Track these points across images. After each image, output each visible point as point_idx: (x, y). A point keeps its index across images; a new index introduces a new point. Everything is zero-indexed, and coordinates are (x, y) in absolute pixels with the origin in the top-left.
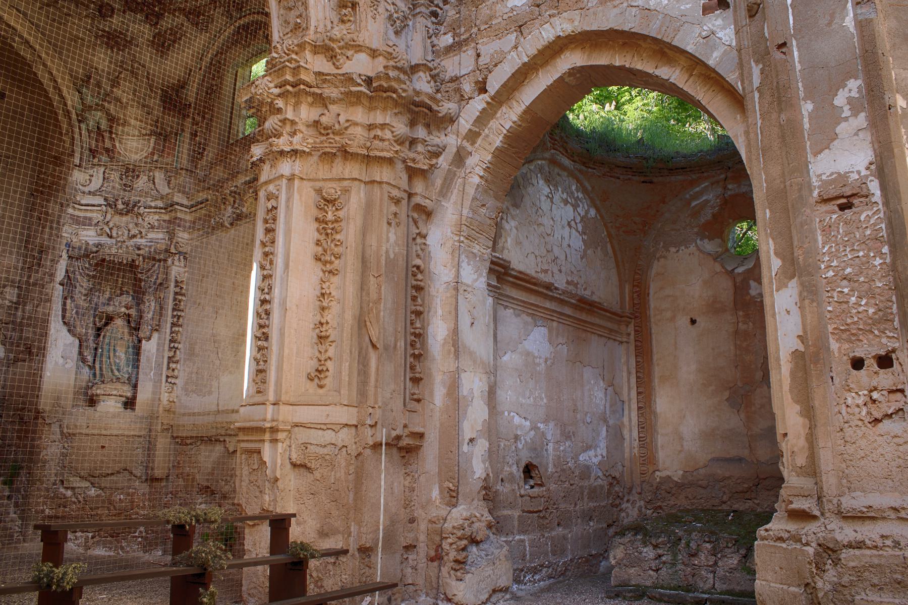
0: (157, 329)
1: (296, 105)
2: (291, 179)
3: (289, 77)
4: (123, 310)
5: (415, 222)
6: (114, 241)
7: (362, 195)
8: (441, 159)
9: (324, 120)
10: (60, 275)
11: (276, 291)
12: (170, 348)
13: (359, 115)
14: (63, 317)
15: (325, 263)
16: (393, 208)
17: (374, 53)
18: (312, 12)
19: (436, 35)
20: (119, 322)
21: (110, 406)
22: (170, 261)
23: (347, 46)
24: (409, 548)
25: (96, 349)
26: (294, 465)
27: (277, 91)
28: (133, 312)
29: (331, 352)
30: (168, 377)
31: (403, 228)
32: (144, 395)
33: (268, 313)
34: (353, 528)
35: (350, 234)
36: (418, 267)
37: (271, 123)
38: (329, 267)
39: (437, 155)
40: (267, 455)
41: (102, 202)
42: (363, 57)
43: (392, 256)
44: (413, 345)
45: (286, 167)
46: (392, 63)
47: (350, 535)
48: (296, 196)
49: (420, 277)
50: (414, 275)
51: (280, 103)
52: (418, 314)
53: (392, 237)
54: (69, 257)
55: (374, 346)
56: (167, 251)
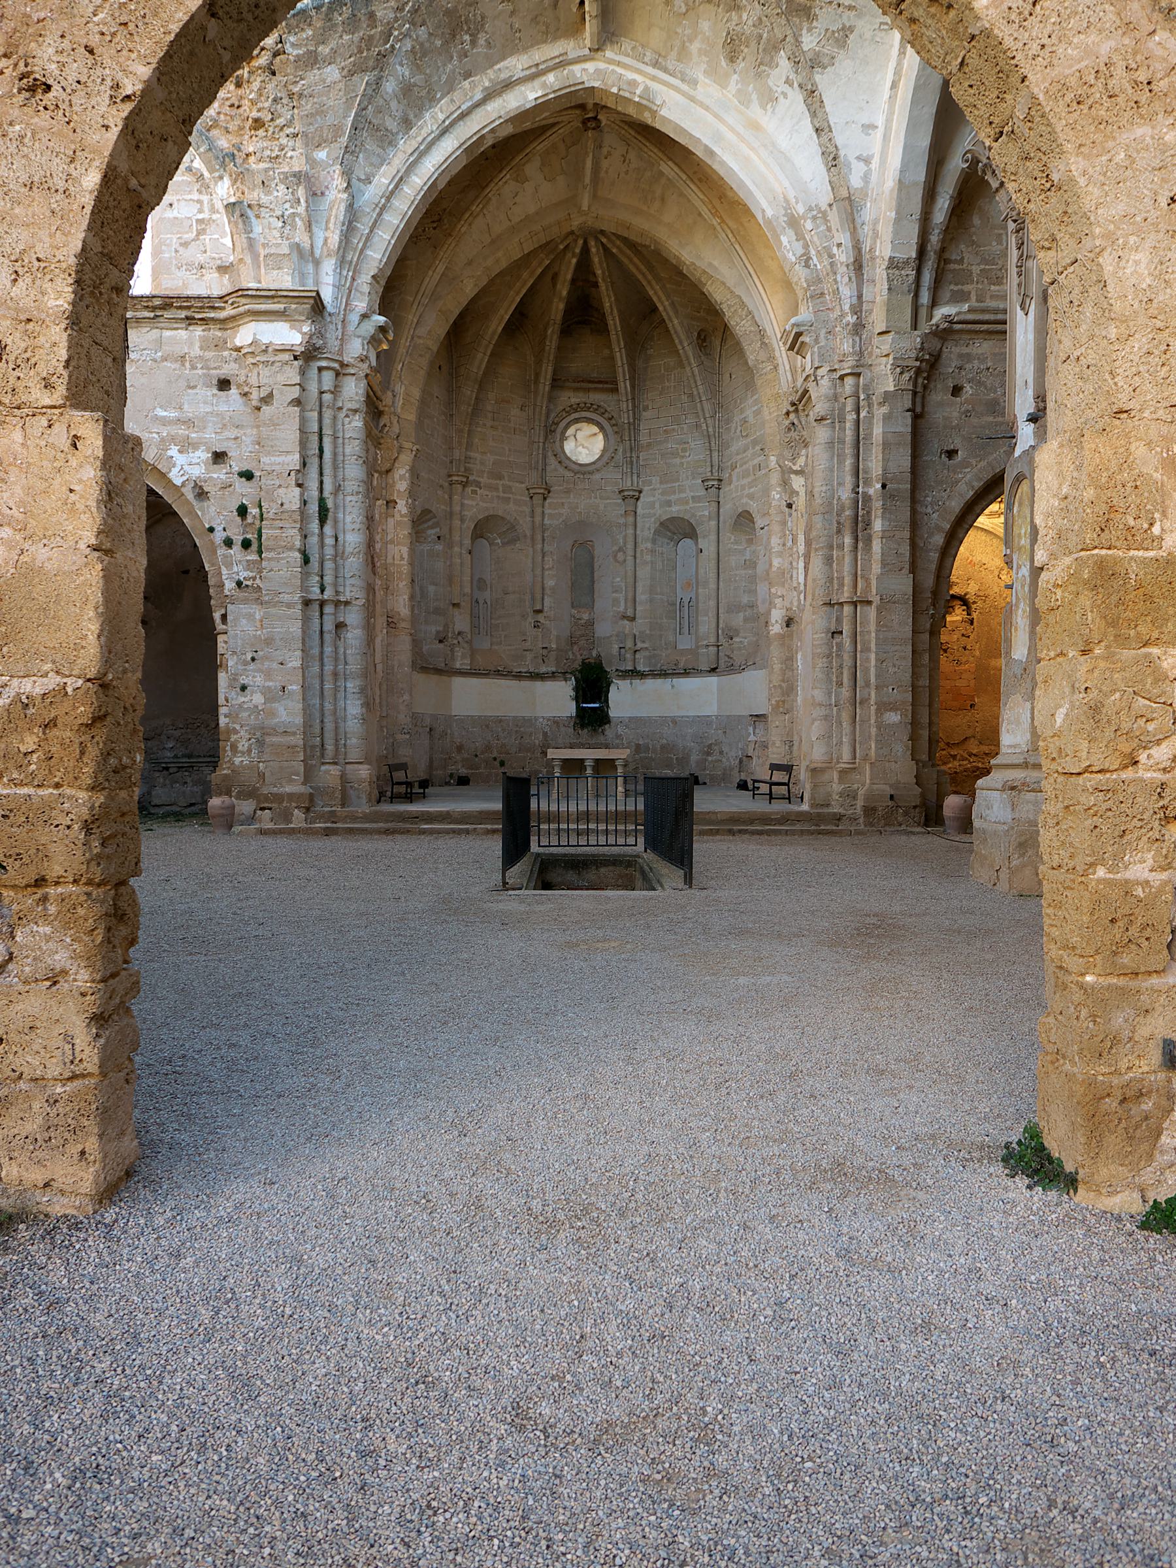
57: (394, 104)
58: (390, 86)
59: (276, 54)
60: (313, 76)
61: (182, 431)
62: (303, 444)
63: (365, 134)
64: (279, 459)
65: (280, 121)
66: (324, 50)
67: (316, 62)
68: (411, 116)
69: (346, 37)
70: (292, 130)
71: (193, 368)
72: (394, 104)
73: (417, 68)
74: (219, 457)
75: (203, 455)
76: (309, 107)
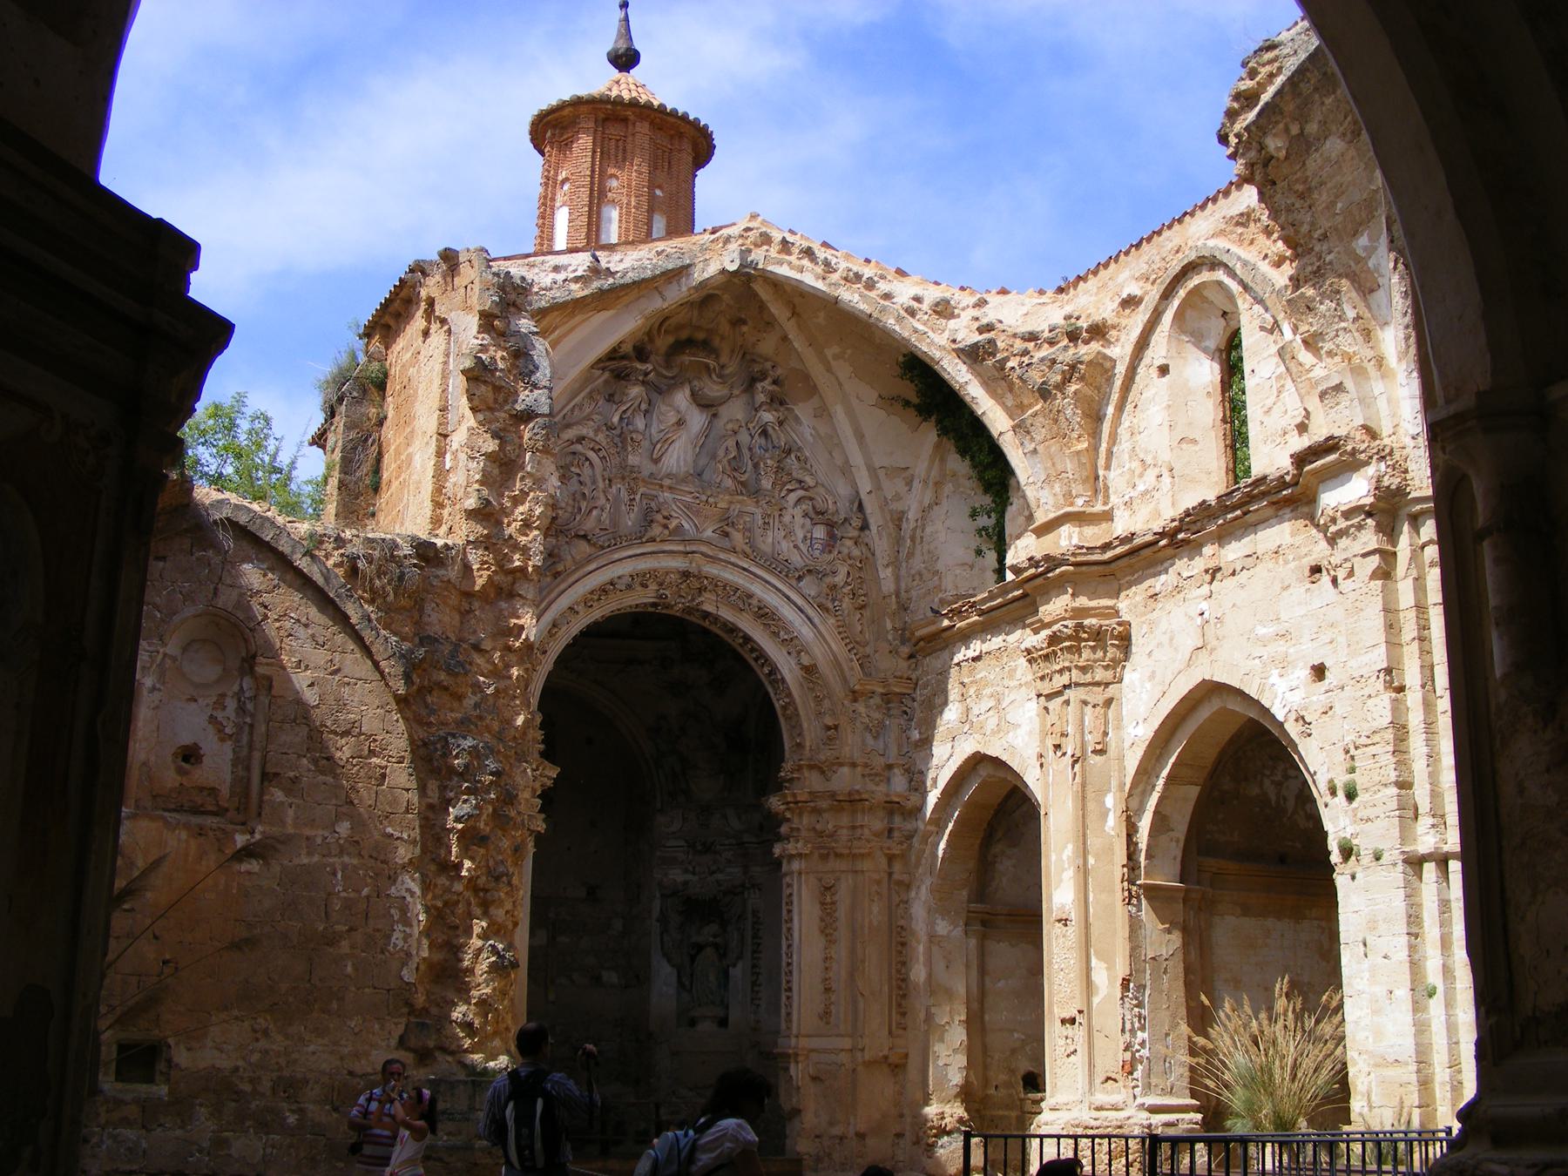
0: (740, 957)
1: (800, 815)
2: (800, 873)
4: (711, 939)
5: (898, 893)
6: (695, 878)
7: (850, 881)
8: (915, 839)
9: (818, 827)
10: (656, 913)
11: (795, 957)
12: (753, 974)
13: (845, 820)
14: (662, 948)
15: (827, 935)
16: (875, 887)
17: (854, 765)
18: (806, 733)
19: (909, 729)
20: (709, 951)
21: (706, 1027)
22: (746, 893)
23: (833, 764)
24: (899, 1135)
25: (692, 975)
26: (815, 1079)
27: (782, 807)
28: (718, 940)
29: (833, 999)
30: (752, 999)
32: (735, 1015)
33: (791, 972)
34: (852, 1120)
35: (842, 911)
36: (902, 927)
37: (784, 829)
38: (829, 938)
39: (912, 837)
40: (793, 1071)
41: (683, 843)
42: (845, 770)
43: (875, 924)
44: (900, 988)
45: (796, 865)
46: (867, 771)
48: (804, 887)
49: (904, 934)
50: (899, 933)
51: (788, 815)
52: (904, 963)
53: (875, 909)
54: (662, 895)
55: (861, 994)
56: (743, 886)
59: (1266, 165)
60: (1313, 162)
61: (1280, 647)
62: (1392, 627)
64: (1365, 659)
65: (1305, 228)
66: (1312, 128)
67: (1309, 145)
69: (1329, 101)
70: (1319, 232)
71: (1286, 562)
74: (1319, 672)
75: (1304, 673)
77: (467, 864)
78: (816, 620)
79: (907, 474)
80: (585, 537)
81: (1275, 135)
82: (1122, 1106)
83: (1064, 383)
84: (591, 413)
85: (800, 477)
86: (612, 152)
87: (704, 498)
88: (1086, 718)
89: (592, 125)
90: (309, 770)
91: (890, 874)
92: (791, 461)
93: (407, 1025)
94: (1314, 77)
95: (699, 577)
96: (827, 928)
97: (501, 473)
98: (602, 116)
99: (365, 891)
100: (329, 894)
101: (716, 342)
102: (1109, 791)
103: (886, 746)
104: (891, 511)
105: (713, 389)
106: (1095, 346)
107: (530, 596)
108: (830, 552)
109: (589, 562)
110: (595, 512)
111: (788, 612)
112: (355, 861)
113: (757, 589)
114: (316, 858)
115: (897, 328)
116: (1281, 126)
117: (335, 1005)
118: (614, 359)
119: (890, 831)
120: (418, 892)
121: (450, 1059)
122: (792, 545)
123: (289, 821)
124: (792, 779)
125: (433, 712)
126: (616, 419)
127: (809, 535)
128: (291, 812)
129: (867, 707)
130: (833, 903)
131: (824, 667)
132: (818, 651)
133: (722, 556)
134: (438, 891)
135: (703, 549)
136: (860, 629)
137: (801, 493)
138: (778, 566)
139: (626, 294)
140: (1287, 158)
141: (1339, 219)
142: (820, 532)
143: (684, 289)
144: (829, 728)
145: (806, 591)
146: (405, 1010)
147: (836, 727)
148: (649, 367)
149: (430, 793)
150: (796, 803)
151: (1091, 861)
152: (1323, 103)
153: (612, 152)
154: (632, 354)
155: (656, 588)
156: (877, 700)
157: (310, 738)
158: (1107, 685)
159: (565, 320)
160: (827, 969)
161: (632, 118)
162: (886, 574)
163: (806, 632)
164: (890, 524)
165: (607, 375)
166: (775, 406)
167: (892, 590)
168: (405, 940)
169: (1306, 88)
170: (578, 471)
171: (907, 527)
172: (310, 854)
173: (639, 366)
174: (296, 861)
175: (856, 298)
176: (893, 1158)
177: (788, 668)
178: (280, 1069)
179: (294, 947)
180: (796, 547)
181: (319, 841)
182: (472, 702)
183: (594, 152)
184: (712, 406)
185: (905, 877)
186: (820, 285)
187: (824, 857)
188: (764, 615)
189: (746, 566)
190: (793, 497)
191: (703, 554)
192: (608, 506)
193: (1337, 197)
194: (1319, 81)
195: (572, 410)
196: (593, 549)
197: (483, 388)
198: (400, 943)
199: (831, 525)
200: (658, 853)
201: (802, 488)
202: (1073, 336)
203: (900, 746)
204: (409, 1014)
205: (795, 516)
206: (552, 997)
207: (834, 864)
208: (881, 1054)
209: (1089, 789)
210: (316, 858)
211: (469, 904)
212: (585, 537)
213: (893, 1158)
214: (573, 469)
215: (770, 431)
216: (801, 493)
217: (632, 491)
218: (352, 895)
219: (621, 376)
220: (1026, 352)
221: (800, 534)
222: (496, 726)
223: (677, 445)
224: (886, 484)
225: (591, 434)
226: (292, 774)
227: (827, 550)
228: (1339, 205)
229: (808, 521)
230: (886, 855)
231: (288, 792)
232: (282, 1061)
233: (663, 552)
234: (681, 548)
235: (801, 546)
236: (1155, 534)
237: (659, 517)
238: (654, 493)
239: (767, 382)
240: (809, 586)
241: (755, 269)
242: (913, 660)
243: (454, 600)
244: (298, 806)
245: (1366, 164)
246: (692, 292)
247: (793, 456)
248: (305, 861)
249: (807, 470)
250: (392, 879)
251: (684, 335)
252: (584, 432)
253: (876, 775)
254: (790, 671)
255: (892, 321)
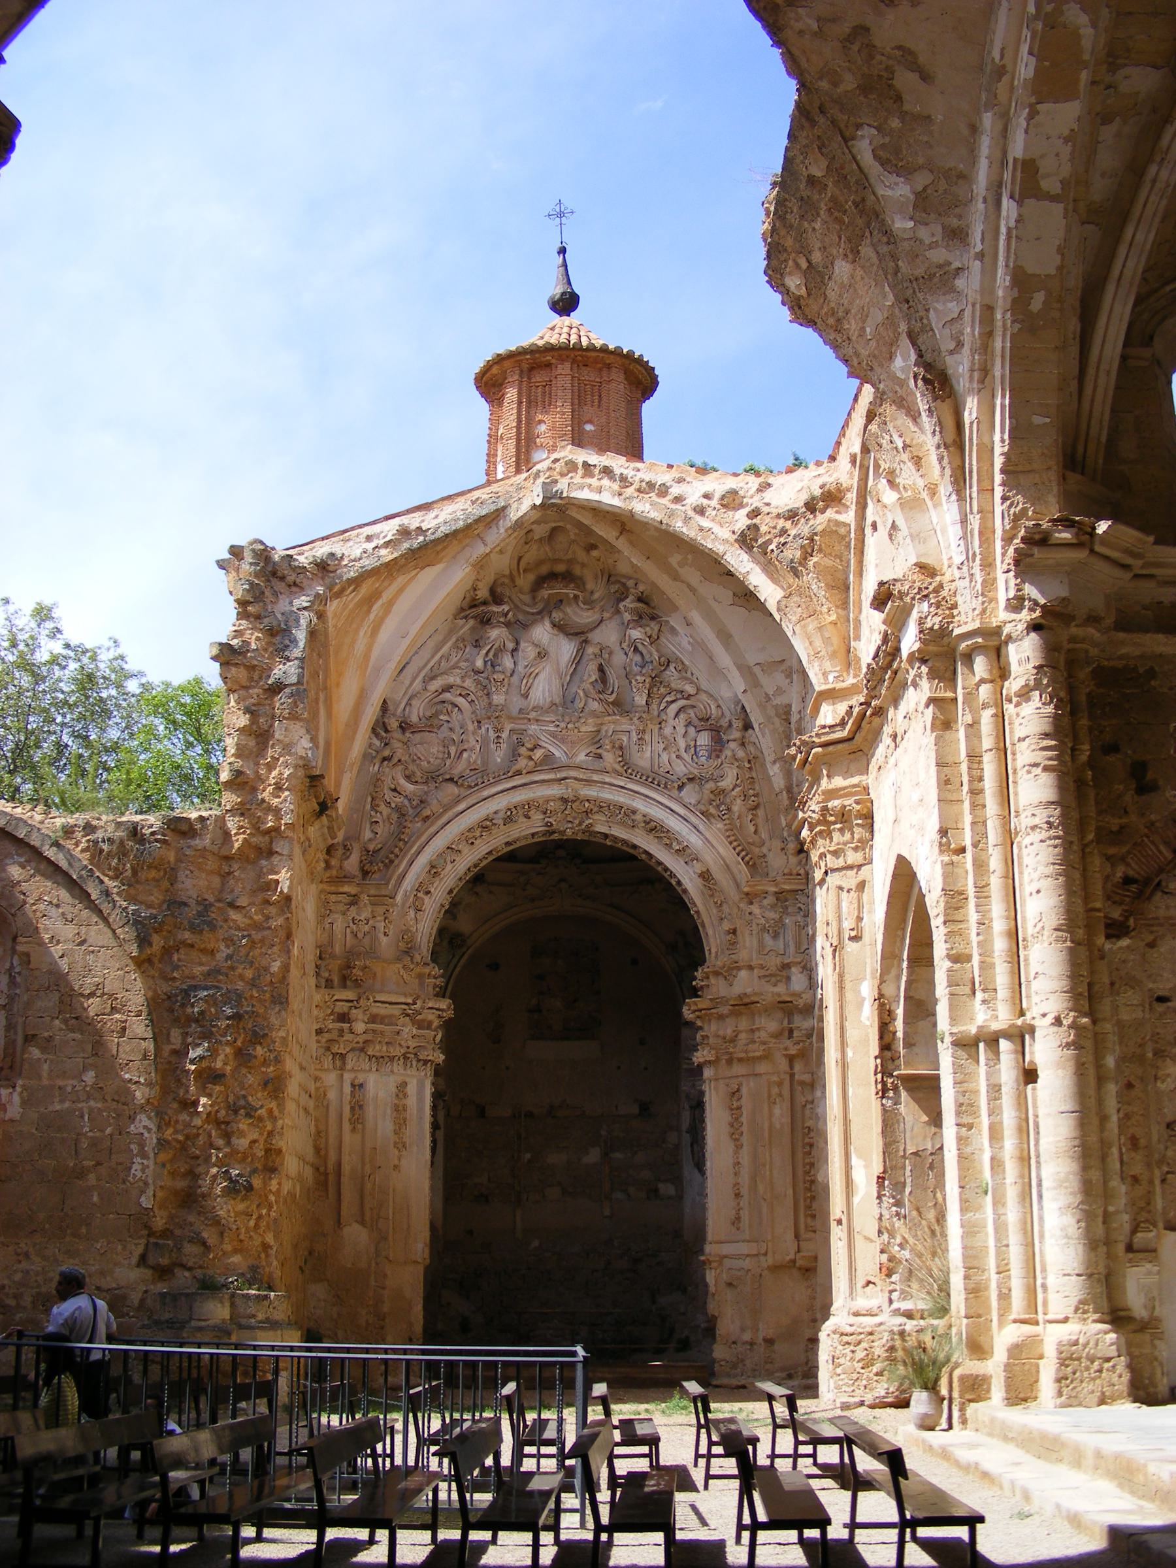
3: (693, 1008)
7: (752, 1084)
13: (744, 1024)
16: (775, 1090)
17: (751, 968)
23: (733, 969)
26: (730, 1285)
31: (787, 1104)
34: (760, 1326)
43: (778, 1126)
46: (763, 972)
47: (757, 1330)
51: (699, 1023)
52: (812, 1165)
57: (923, 233)
58: (901, 224)
63: (920, 296)
68: (955, 222)
72: (923, 233)
73: (905, 171)
76: (854, 327)
77: (203, 1100)
78: (701, 827)
79: (783, 667)
80: (451, 780)
81: (790, 274)
82: (875, 1311)
83: (805, 559)
84: (458, 661)
85: (679, 687)
86: (539, 398)
87: (563, 725)
88: (844, 905)
89: (516, 377)
90: (61, 1030)
91: (792, 1076)
92: (671, 674)
93: (147, 1245)
94: (794, 205)
95: (577, 799)
96: (735, 1134)
97: (258, 744)
98: (525, 366)
99: (108, 1131)
100: (78, 1134)
101: (577, 571)
102: (864, 979)
103: (786, 946)
104: (776, 707)
105: (582, 616)
106: (830, 513)
107: (285, 852)
108: (718, 757)
109: (458, 802)
110: (465, 755)
111: (673, 823)
112: (99, 1105)
113: (639, 804)
114: (67, 1105)
115: (684, 530)
116: (791, 263)
117: (84, 1230)
118: (475, 606)
119: (791, 1031)
120: (154, 1129)
121: (187, 1274)
122: (674, 756)
123: (45, 1074)
124: (702, 987)
125: (177, 968)
126: (479, 663)
127: (692, 744)
128: (46, 1067)
129: (761, 907)
130: (739, 1108)
131: (717, 873)
132: (709, 858)
133: (595, 777)
134: (180, 1127)
135: (573, 773)
136: (752, 829)
137: (682, 703)
138: (655, 779)
139: (445, 548)
140: (809, 295)
141: (873, 344)
142: (704, 739)
143: (502, 530)
144: (729, 932)
145: (687, 800)
146: (145, 1232)
147: (734, 932)
148: (506, 608)
149: (173, 1040)
150: (700, 1010)
151: (850, 1053)
152: (814, 229)
153: (539, 398)
154: (490, 599)
155: (542, 816)
156: (771, 900)
157: (61, 1002)
158: (860, 867)
159: (385, 584)
160: (736, 1174)
161: (553, 361)
162: (775, 770)
163: (694, 840)
164: (777, 721)
165: (471, 622)
166: (644, 621)
167: (782, 786)
168: (143, 1171)
169: (793, 218)
170: (446, 718)
171: (794, 718)
172: (62, 1101)
173: (495, 609)
174: (50, 1108)
175: (648, 507)
176: (807, 1363)
177: (687, 877)
178: (38, 1286)
179: (49, 1181)
180: (678, 757)
181: (69, 1089)
182: (224, 955)
183: (520, 403)
184: (583, 633)
185: (806, 1078)
186: (616, 502)
187: (730, 1062)
188: (654, 828)
189: (622, 784)
190: (674, 708)
191: (576, 779)
192: (478, 747)
193: (864, 322)
194: (800, 207)
195: (439, 662)
196: (462, 790)
197: (234, 670)
198: (139, 1174)
199: (717, 733)
200: (685, 1066)
201: (683, 698)
202: (811, 506)
203: (798, 944)
204: (149, 1235)
205: (675, 726)
206: (607, 1212)
207: (738, 1069)
208: (788, 1258)
209: (847, 978)
210: (67, 1105)
211: (210, 1136)
212: (451, 780)
213: (807, 1363)
214: (442, 717)
215: (640, 647)
216: (682, 703)
217: (498, 730)
218: (98, 1134)
219: (485, 621)
220: (784, 531)
221: (682, 744)
222: (249, 974)
223: (541, 677)
224: (764, 679)
225: (458, 681)
226: (46, 1034)
227: (714, 754)
228: (868, 330)
229: (692, 730)
230: (786, 1056)
231: (44, 1050)
232: (40, 1279)
233: (536, 782)
234: (552, 776)
235: (684, 755)
236: (861, 704)
237: (523, 751)
238: (523, 727)
239: (628, 600)
240: (690, 794)
241: (561, 498)
242: (802, 855)
243: (212, 864)
244: (52, 1061)
245: (875, 280)
246: (510, 532)
247: (672, 667)
248: (58, 1107)
249: (686, 679)
250: (132, 1118)
251: (544, 570)
252: (451, 680)
253: (771, 975)
254: (691, 880)
255: (679, 524)
